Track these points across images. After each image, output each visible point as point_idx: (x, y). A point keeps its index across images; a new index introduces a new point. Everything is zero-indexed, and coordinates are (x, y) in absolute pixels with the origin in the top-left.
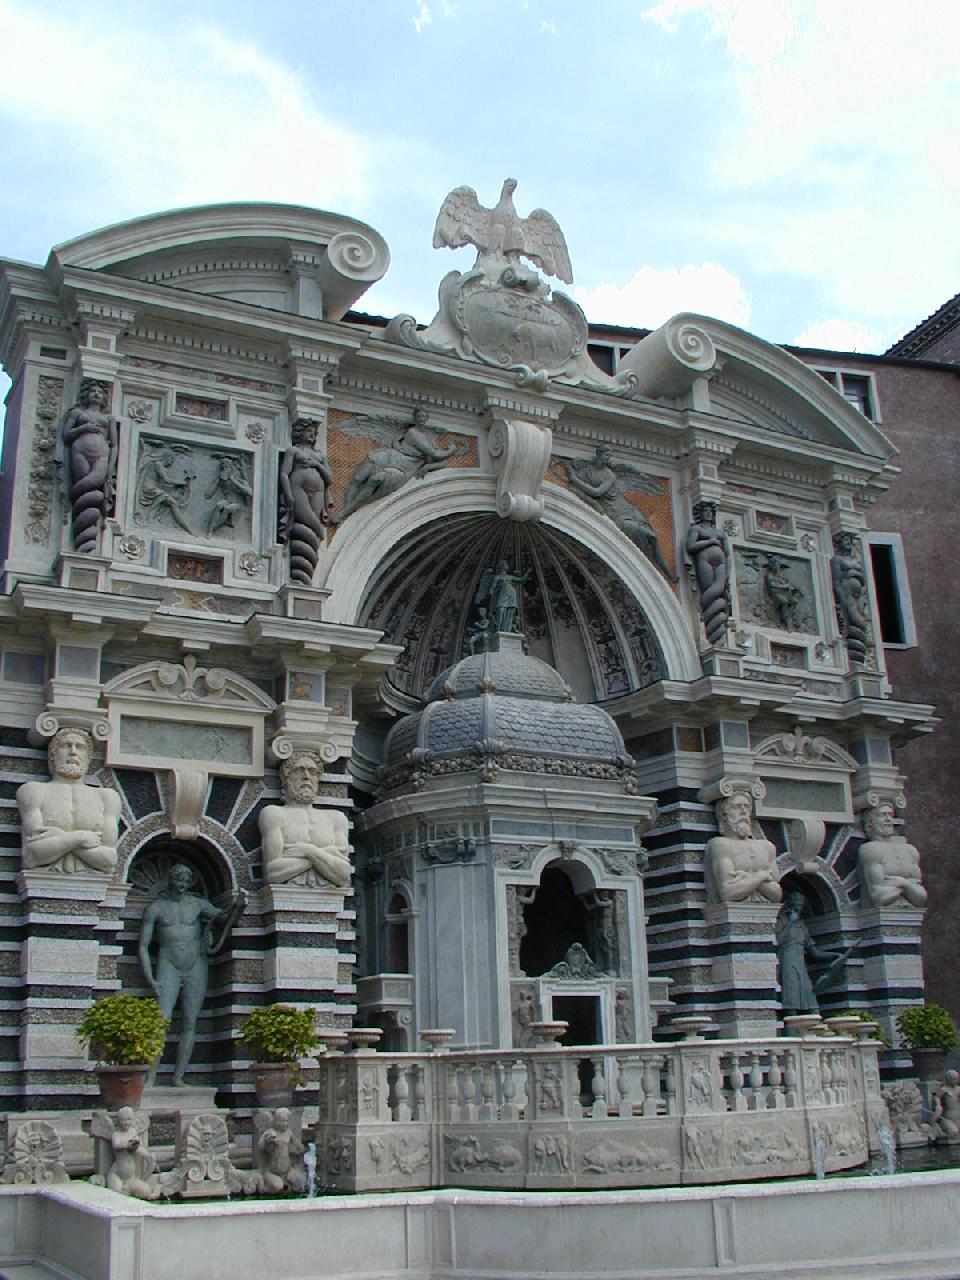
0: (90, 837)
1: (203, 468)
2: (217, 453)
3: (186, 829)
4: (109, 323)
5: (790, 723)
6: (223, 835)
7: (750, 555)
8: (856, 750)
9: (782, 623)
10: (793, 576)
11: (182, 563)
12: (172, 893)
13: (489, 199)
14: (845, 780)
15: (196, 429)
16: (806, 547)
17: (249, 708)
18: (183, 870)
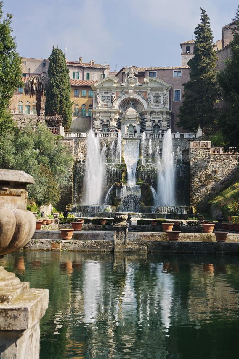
0: (98, 124)
1: (106, 97)
2: (107, 96)
3: (105, 123)
4: (98, 89)
5: (155, 112)
6: (108, 124)
7: (155, 97)
8: (162, 114)
9: (157, 103)
10: (160, 98)
11: (105, 105)
12: (105, 127)
14: (162, 117)
16: (161, 95)
17: (109, 115)
18: (106, 126)
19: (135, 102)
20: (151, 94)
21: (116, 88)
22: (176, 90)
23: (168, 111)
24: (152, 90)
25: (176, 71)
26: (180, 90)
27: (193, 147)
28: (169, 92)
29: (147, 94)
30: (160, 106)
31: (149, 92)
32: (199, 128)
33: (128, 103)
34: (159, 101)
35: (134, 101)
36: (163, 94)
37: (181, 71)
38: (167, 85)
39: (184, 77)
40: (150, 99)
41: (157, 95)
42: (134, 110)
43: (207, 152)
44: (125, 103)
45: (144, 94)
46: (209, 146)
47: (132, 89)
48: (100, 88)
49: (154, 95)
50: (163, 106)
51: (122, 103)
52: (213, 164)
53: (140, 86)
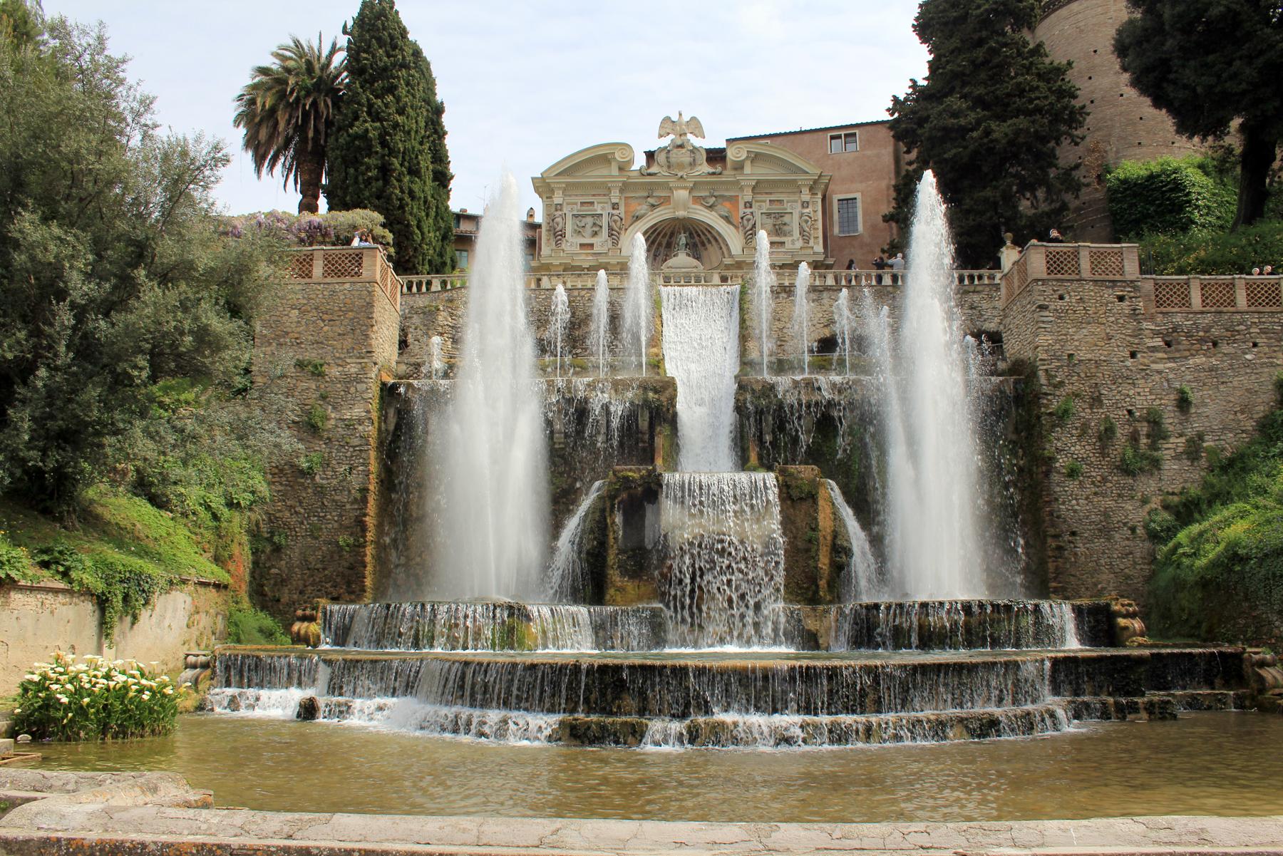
1: (589, 220)
2: (593, 216)
7: (769, 215)
9: (778, 235)
10: (786, 219)
13: (675, 118)
15: (586, 210)
19: (697, 239)
20: (755, 205)
21: (624, 183)
23: (821, 258)
24: (757, 187)
25: (839, 137)
26: (858, 195)
27: (1045, 276)
28: (820, 196)
29: (741, 205)
30: (788, 246)
31: (748, 195)
32: (1009, 243)
33: (669, 245)
34: (785, 228)
36: (799, 204)
37: (854, 135)
38: (814, 171)
39: (868, 153)
40: (751, 223)
41: (776, 208)
42: (695, 262)
43: (1121, 299)
45: (727, 204)
46: (1131, 268)
47: (685, 188)
48: (568, 184)
49: (766, 207)
50: (799, 244)
53: (714, 174)
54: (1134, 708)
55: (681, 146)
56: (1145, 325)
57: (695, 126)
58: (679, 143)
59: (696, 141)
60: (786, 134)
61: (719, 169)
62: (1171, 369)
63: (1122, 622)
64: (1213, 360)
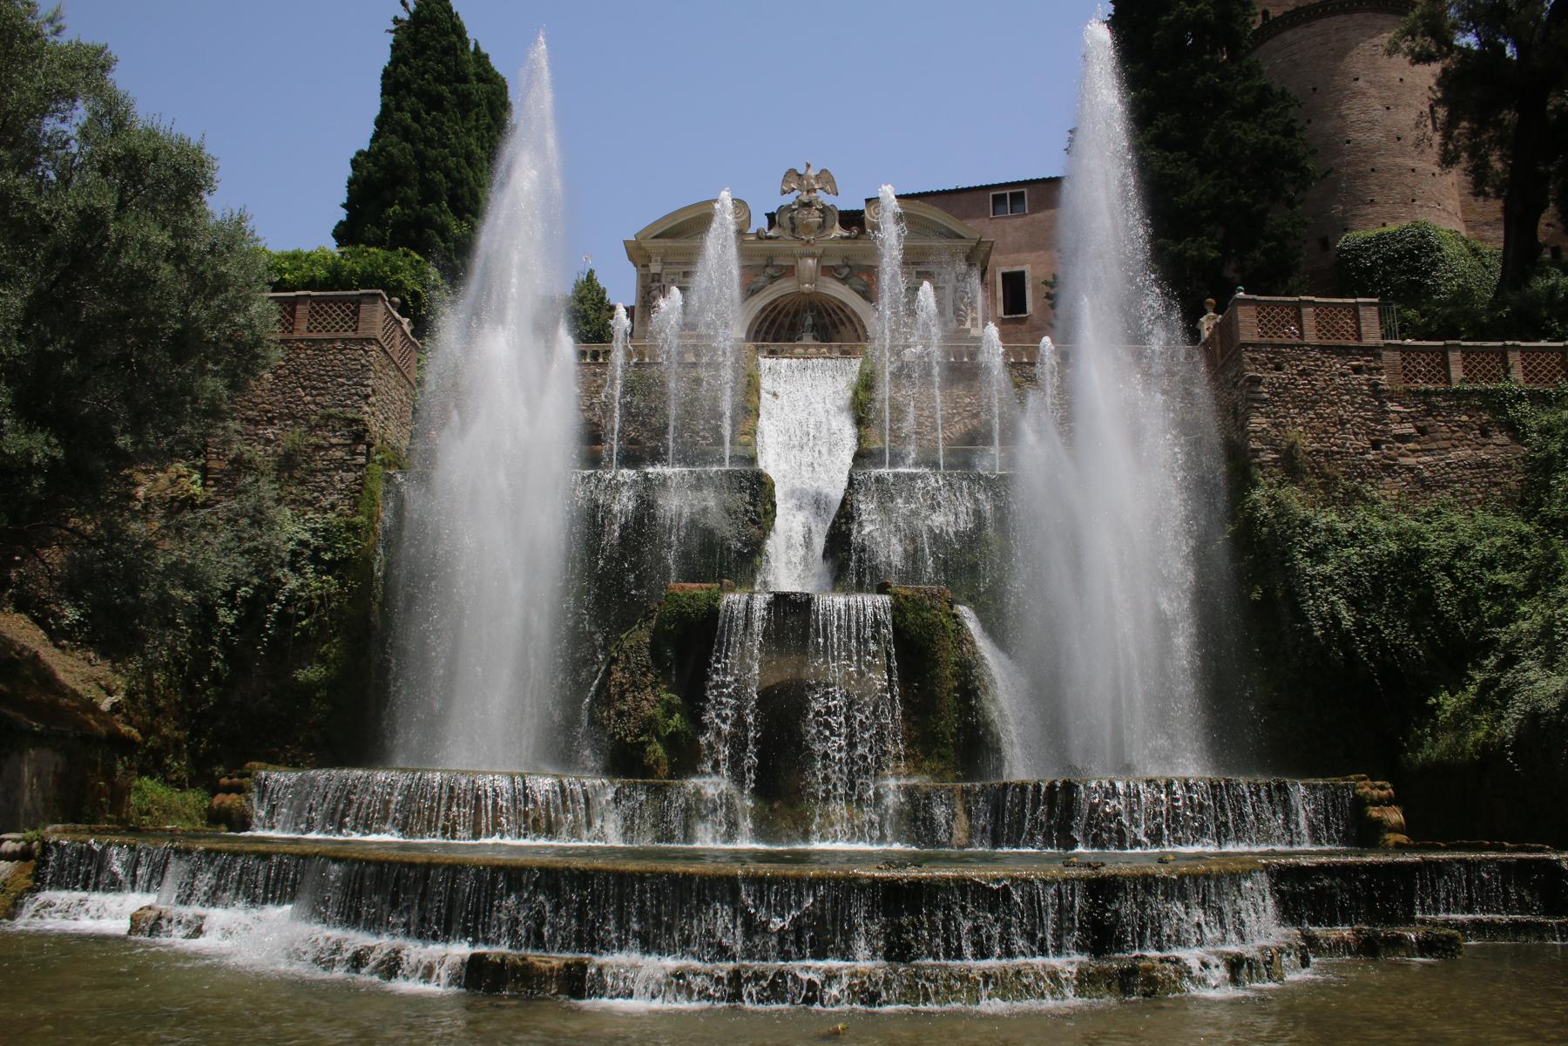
19: (827, 319)
22: (1006, 270)
26: (1027, 268)
27: (1256, 339)
35: (819, 313)
43: (1357, 370)
44: (781, 326)
47: (812, 256)
51: (765, 320)
52: (1411, 461)
54: (1397, 943)
55: (808, 205)
56: (1390, 406)
57: (825, 177)
58: (805, 198)
59: (826, 199)
60: (938, 192)
61: (855, 231)
62: (1427, 465)
63: (1374, 812)
64: (1481, 453)
